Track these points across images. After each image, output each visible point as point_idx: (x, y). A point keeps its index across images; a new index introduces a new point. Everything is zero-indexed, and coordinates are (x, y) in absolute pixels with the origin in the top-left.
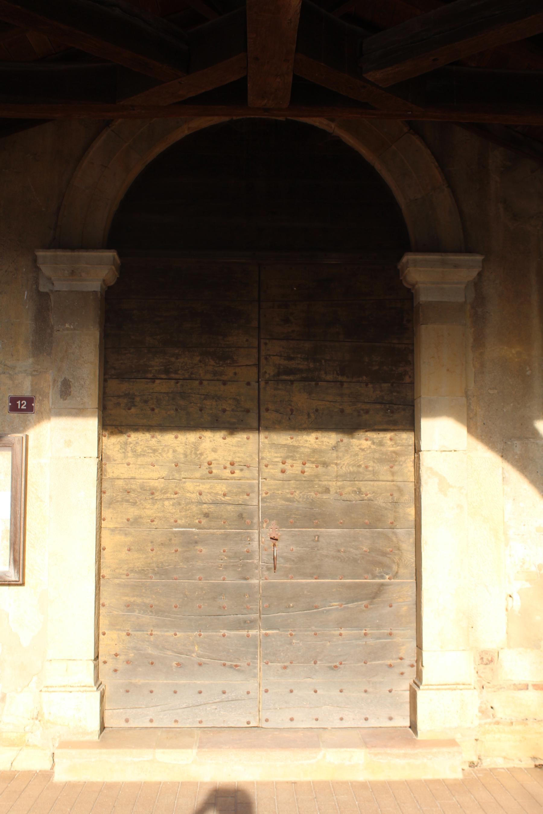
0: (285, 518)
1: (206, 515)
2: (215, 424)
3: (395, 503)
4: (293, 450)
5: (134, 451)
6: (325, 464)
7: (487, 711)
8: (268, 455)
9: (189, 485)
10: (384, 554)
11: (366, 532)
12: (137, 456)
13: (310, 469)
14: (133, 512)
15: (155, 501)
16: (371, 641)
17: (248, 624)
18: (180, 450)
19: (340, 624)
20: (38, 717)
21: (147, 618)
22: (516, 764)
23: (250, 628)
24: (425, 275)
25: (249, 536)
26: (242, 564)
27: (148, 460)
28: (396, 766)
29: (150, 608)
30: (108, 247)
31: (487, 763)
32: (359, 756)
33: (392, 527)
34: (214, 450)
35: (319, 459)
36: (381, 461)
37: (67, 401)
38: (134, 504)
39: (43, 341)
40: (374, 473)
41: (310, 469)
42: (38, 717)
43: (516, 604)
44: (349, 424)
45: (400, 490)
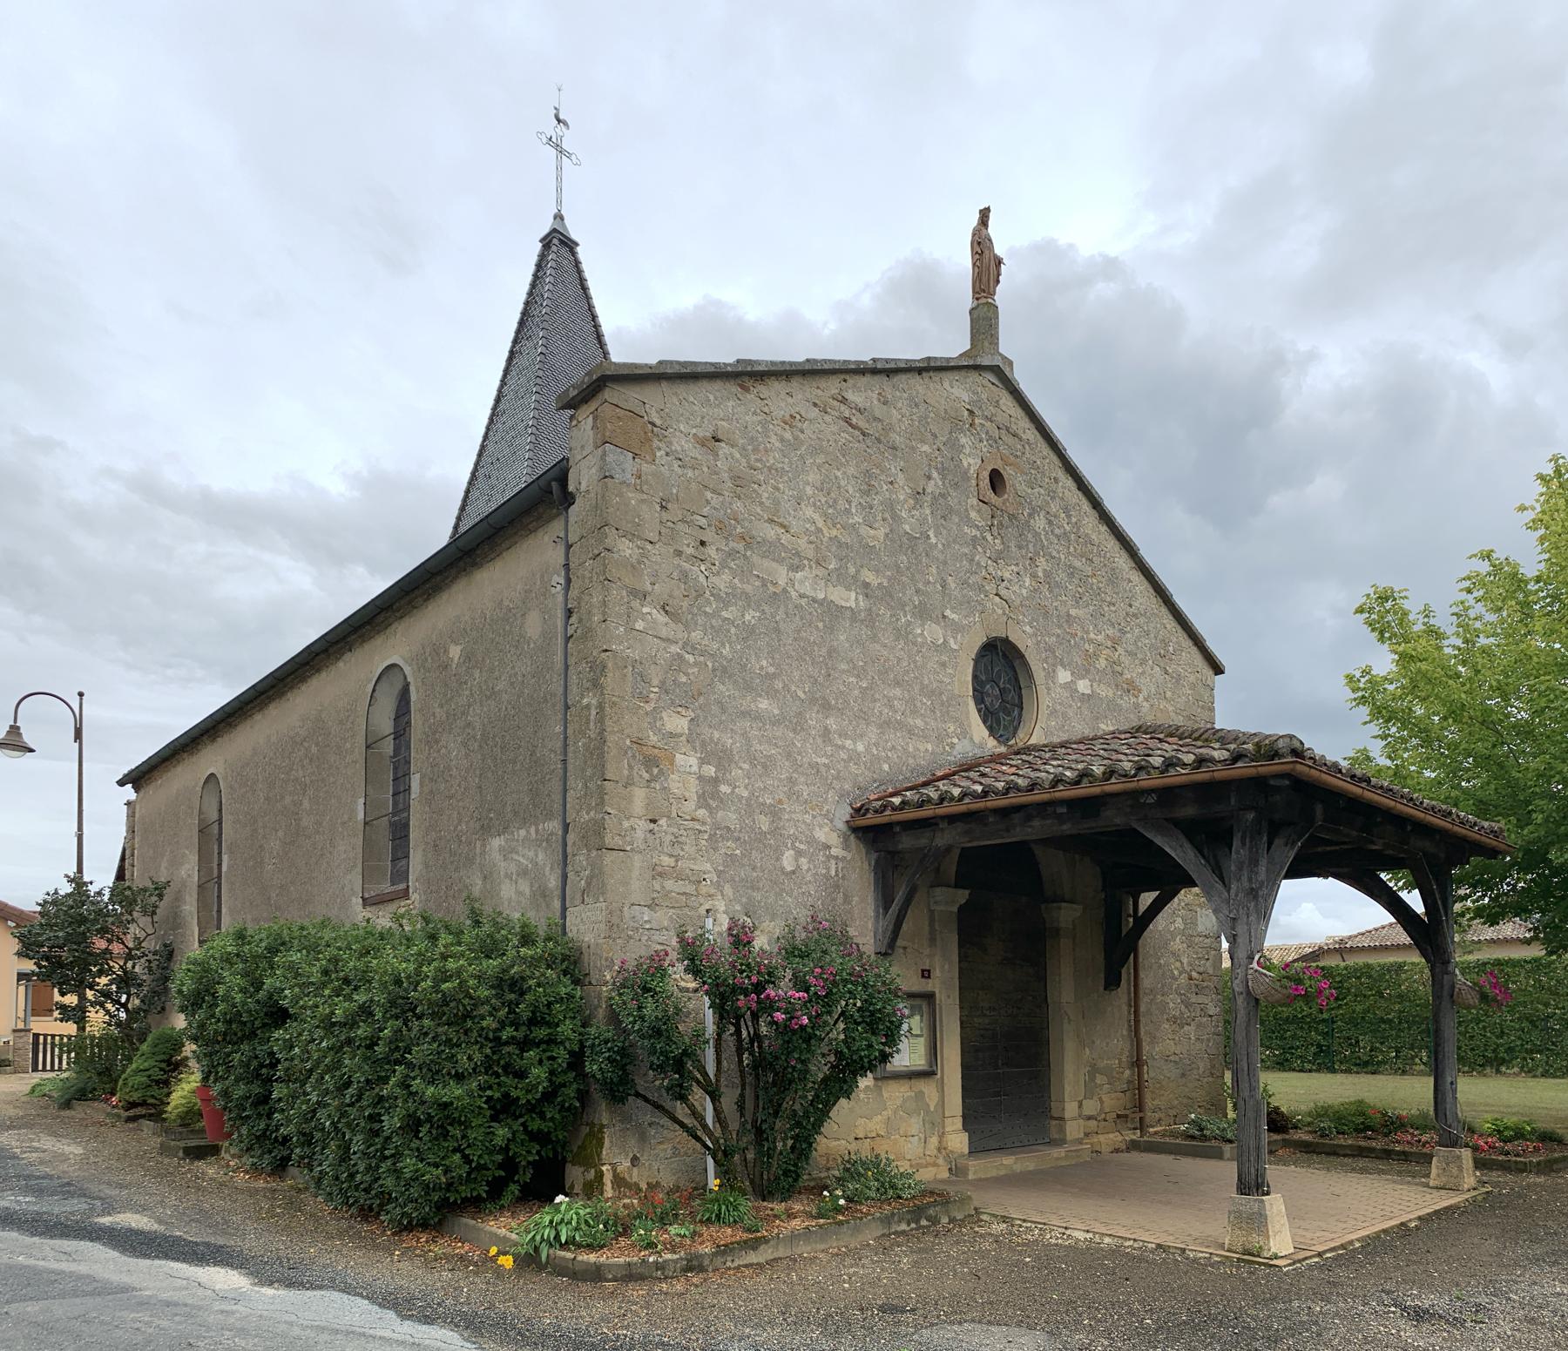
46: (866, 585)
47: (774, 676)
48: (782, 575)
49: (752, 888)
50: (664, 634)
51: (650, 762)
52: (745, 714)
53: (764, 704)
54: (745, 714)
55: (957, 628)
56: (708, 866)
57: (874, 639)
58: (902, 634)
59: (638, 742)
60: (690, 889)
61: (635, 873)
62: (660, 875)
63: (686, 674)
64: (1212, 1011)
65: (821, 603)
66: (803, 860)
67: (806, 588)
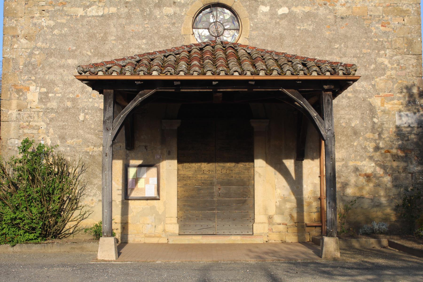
0: (222, 183)
1: (203, 183)
2: (205, 161)
3: (249, 180)
4: (224, 167)
5: (185, 168)
6: (232, 170)
7: (271, 230)
8: (218, 168)
9: (199, 176)
10: (246, 192)
11: (242, 187)
12: (186, 169)
13: (228, 172)
14: (185, 182)
15: (190, 180)
16: (243, 214)
17: (213, 209)
18: (196, 167)
19: (236, 209)
20: (164, 230)
21: (189, 208)
22: (277, 242)
23: (214, 210)
24: (255, 124)
25: (213, 188)
26: (212, 195)
27: (188, 170)
28: (248, 240)
29: (189, 206)
31: (270, 241)
32: (239, 238)
33: (248, 186)
34: (205, 167)
35: (230, 169)
36: (245, 170)
37: (169, 157)
38: (185, 180)
39: (163, 142)
40: (244, 172)
41: (228, 172)
42: (164, 230)
43: (278, 204)
44: (237, 161)
45: (250, 177)
47: (76, 50)
48: (81, 12)
49: (63, 129)
50: (26, 46)
51: (18, 91)
53: (70, 61)
54: (60, 67)
55: (182, 6)
56: (43, 123)
57: (130, 23)
58: (150, 17)
59: (15, 85)
60: (35, 132)
61: (12, 128)
62: (22, 128)
63: (35, 58)
65: (102, 16)
66: (87, 116)
67: (94, 13)
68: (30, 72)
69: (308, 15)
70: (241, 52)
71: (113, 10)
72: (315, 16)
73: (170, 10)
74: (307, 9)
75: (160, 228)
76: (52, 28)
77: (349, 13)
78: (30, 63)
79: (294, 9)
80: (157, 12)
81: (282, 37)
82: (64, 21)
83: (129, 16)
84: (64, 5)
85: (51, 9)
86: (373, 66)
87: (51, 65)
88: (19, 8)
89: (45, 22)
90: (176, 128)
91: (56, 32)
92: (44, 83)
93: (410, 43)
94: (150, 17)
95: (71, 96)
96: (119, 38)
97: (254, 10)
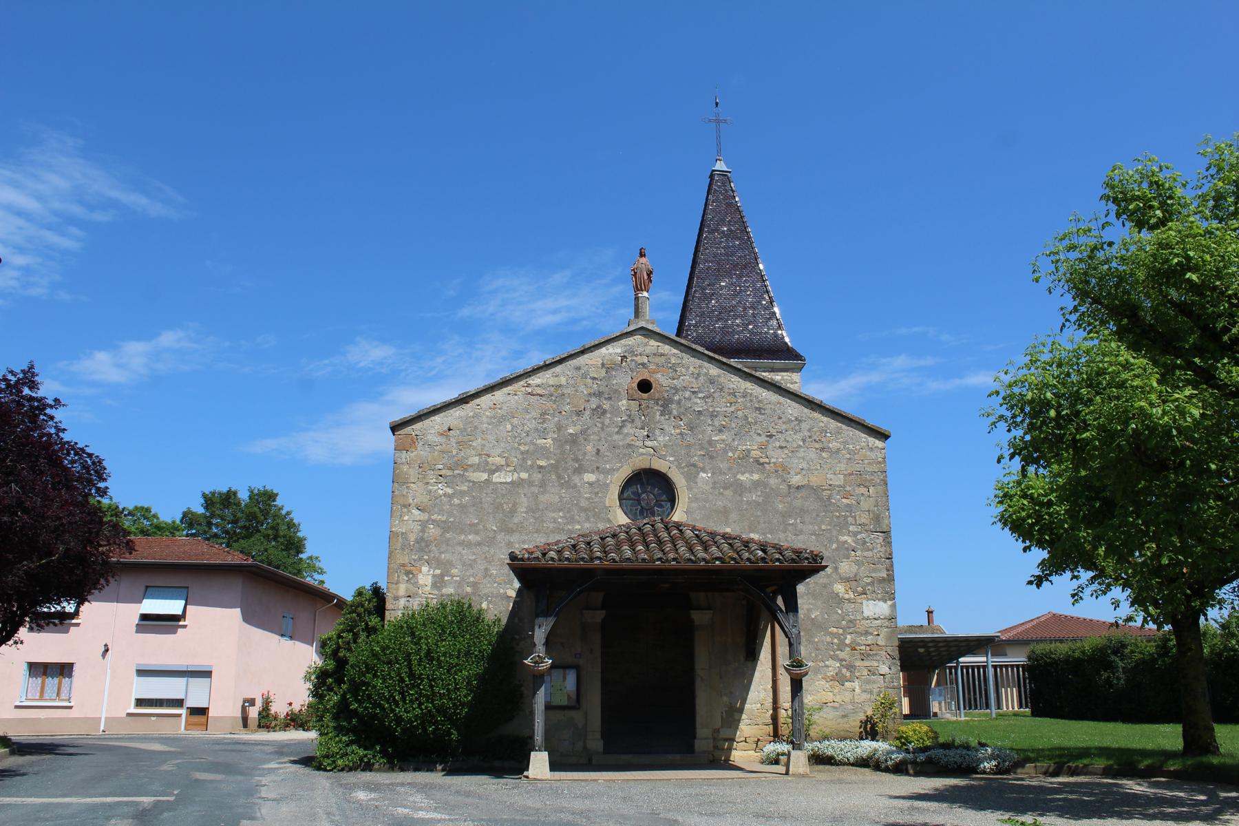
20: (585, 747)
24: (698, 617)
30: (602, 609)
46: (541, 467)
48: (485, 476)
51: (408, 573)
52: (461, 543)
58: (568, 485)
64: (884, 669)
65: (512, 482)
68: (421, 550)
69: (756, 484)
70: (689, 533)
71: (524, 475)
72: (765, 485)
73: (590, 477)
74: (756, 477)
75: (580, 745)
76: (450, 496)
77: (805, 482)
78: (422, 539)
79: (740, 477)
80: (576, 479)
81: (725, 512)
82: (465, 488)
83: (543, 484)
84: (465, 470)
85: (449, 473)
86: (834, 546)
87: (447, 542)
88: (411, 472)
89: (442, 489)
90: (599, 620)
91: (456, 501)
92: (439, 563)
93: (877, 519)
94: (568, 485)
95: (472, 579)
96: (530, 510)
97: (691, 478)
